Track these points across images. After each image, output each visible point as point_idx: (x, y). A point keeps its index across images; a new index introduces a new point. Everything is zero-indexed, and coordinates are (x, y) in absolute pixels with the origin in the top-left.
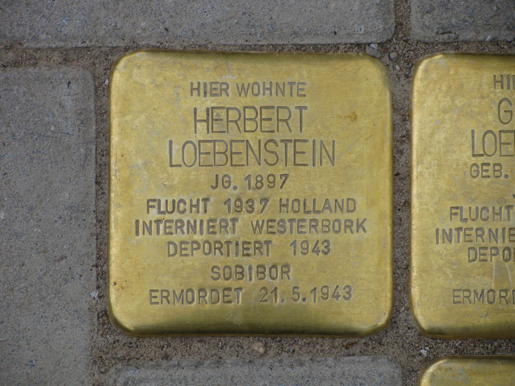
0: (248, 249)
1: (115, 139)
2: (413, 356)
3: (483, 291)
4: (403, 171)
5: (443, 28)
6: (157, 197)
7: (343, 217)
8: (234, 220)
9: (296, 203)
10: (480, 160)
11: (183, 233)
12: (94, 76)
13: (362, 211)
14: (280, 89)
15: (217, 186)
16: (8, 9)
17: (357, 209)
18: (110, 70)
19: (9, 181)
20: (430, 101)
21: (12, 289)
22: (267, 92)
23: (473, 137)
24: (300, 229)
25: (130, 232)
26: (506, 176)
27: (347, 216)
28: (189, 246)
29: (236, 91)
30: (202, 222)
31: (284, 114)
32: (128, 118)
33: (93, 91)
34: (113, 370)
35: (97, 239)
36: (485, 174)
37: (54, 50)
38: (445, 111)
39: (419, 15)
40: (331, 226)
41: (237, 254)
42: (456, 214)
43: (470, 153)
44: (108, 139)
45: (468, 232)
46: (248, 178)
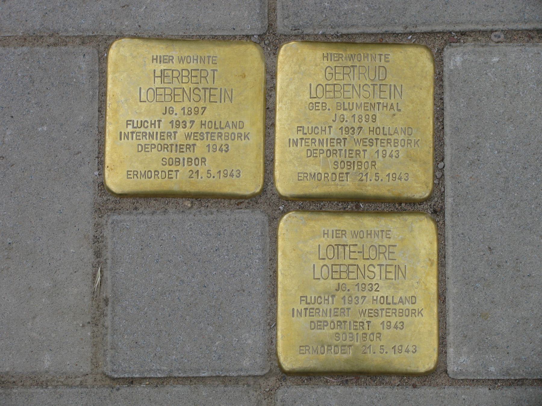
0: (183, 148)
1: (109, 86)
2: (275, 210)
3: (315, 173)
4: (271, 106)
5: (295, 27)
6: (132, 119)
7: (236, 131)
8: (175, 133)
9: (210, 124)
10: (314, 100)
11: (146, 139)
12: (98, 52)
13: (247, 128)
14: (202, 60)
15: (166, 113)
16: (51, 14)
17: (245, 127)
18: (107, 48)
19: (50, 109)
20: (287, 67)
21: (50, 170)
22: (195, 61)
23: (311, 88)
24: (212, 138)
25: (117, 138)
26: (329, 109)
27: (239, 131)
28: (149, 147)
29: (178, 60)
30: (157, 133)
31: (204, 74)
32: (117, 75)
33: (97, 59)
34: (106, 216)
35: (98, 142)
36: (317, 108)
37: (76, 37)
38: (295, 73)
39: (281, 19)
40: (230, 136)
41: (176, 151)
42: (300, 130)
43: (309, 96)
44: (106, 86)
45: (307, 141)
46: (183, 109)
